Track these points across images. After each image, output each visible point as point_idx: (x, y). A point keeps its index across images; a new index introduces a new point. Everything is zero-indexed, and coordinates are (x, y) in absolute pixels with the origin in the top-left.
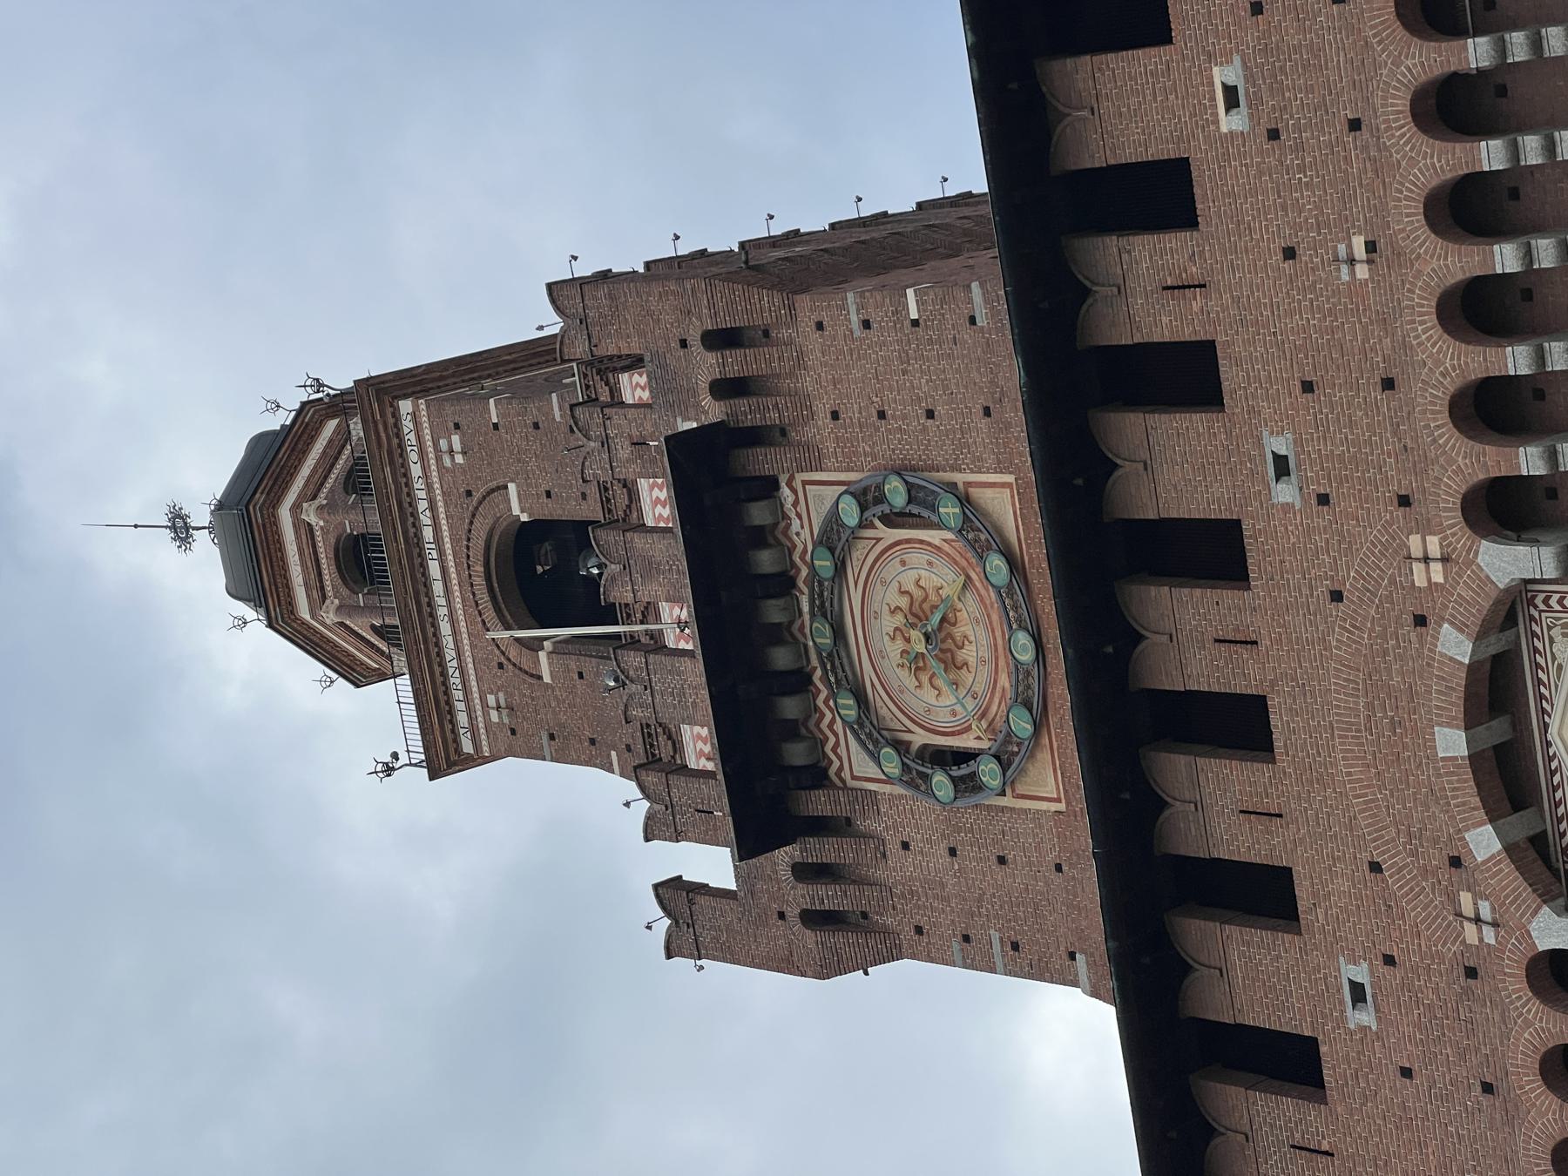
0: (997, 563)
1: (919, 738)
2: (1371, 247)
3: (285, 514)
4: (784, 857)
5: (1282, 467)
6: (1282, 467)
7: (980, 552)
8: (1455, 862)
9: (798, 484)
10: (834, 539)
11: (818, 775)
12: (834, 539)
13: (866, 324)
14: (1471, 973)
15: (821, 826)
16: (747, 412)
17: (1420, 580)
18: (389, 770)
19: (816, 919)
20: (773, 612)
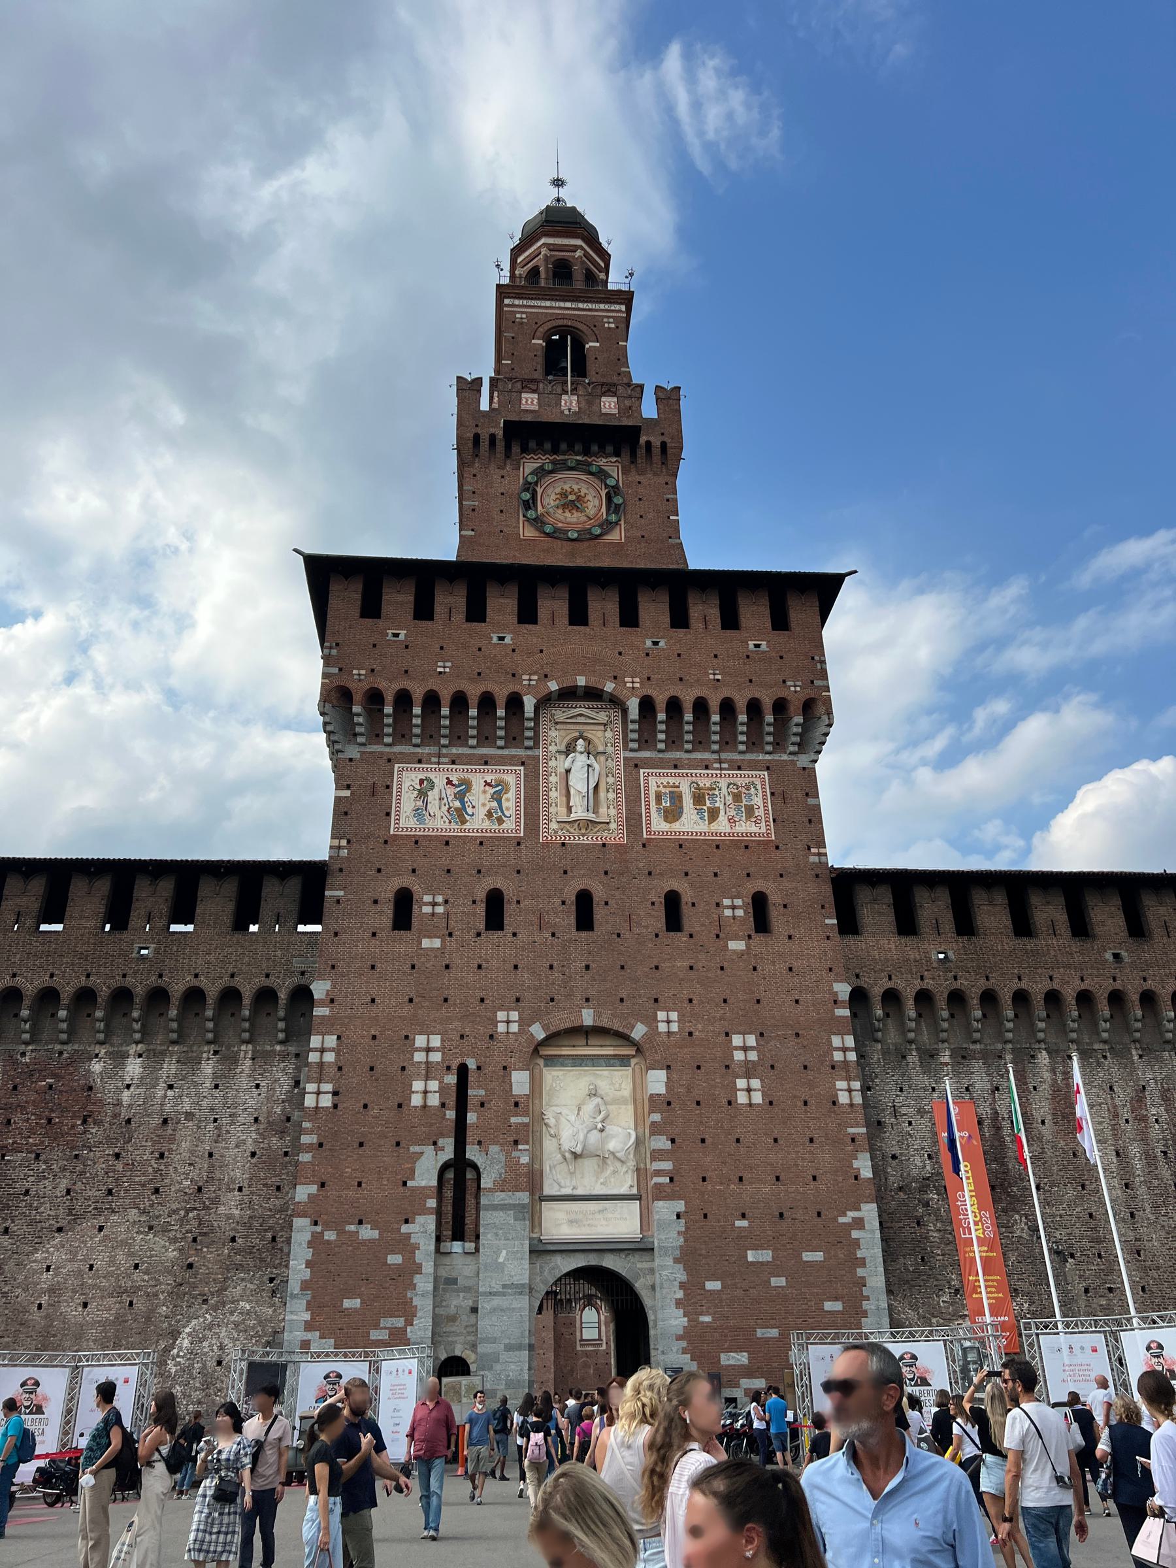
0: (598, 531)
1: (539, 490)
2: (718, 680)
3: (579, 242)
4: (500, 433)
5: (656, 643)
6: (656, 643)
7: (601, 526)
8: (546, 676)
9: (617, 464)
10: (602, 475)
11: (525, 450)
12: (602, 475)
13: (668, 500)
14: (514, 675)
15: (508, 448)
16: (641, 452)
17: (626, 679)
18: (498, 266)
19: (477, 437)
20: (579, 447)
